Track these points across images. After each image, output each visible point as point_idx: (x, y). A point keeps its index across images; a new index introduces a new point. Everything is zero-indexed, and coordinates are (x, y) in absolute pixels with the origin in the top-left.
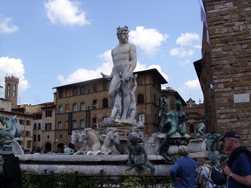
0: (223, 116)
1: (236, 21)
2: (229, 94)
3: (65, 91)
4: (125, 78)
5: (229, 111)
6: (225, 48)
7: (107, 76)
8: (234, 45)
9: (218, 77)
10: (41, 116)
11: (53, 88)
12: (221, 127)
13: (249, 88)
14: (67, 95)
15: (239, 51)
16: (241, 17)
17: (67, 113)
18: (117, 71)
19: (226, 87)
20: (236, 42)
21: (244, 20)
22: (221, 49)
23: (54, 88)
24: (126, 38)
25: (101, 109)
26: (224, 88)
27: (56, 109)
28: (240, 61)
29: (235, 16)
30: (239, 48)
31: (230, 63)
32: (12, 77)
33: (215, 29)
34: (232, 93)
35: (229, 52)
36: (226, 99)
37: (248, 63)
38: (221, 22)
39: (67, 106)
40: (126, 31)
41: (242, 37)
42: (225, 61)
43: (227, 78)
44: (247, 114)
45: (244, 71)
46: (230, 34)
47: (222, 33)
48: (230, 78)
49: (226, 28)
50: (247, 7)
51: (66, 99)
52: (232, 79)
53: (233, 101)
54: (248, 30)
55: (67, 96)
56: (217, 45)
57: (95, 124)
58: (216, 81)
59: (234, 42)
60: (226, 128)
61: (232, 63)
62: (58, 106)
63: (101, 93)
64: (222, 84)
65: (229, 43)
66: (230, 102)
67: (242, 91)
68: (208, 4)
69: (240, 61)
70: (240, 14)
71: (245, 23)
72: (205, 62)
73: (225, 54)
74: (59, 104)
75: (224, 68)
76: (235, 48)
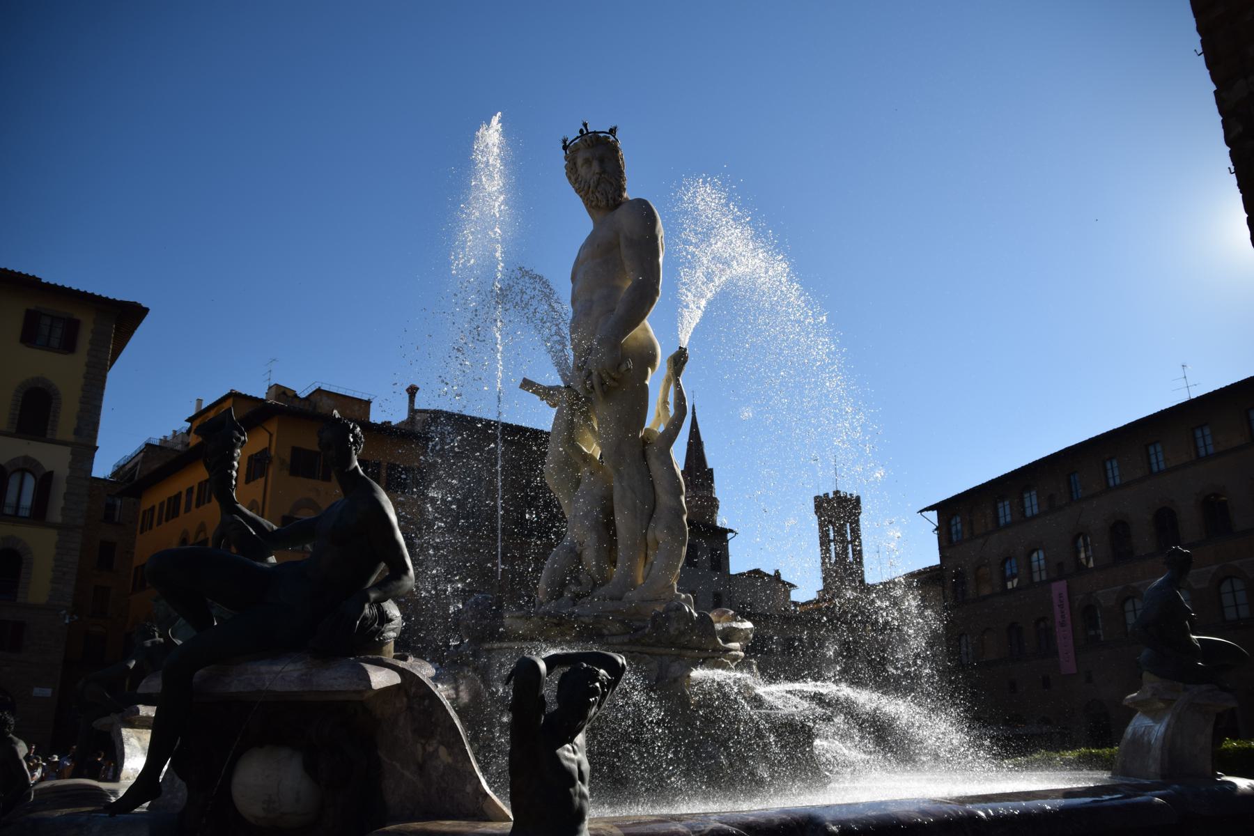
11: (921, 511)
32: (836, 492)
57: (1092, 633)
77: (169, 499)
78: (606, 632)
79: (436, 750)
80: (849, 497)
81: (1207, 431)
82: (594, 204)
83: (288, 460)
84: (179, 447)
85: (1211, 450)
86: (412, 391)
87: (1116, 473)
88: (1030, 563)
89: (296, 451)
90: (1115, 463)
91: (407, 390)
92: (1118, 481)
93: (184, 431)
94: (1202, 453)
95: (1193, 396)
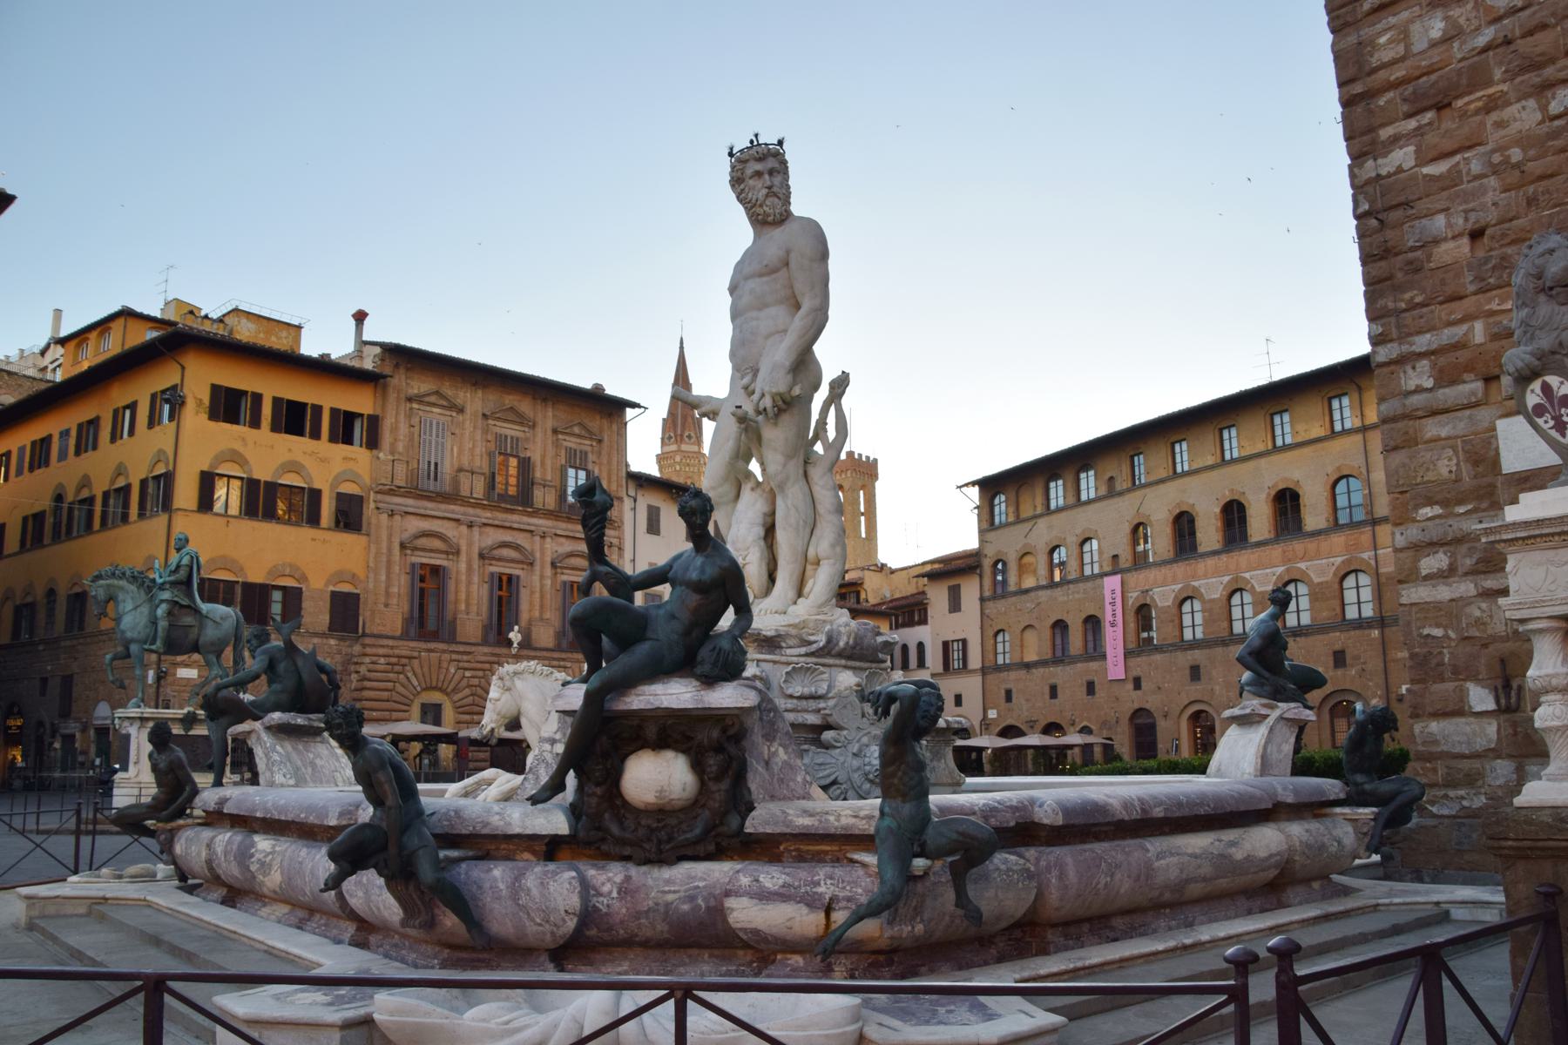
0: (1434, 562)
2: (1470, 417)
3: (1014, 493)
6: (1431, 138)
7: (710, 399)
8: (1495, 108)
9: (1398, 327)
10: (926, 610)
11: (960, 487)
12: (1426, 631)
14: (1022, 507)
15: (1524, 141)
17: (1027, 591)
19: (1446, 378)
22: (1411, 149)
23: (966, 485)
24: (767, 196)
25: (1165, 563)
26: (1440, 383)
27: (981, 576)
28: (1531, 202)
31: (1469, 226)
33: (1372, 43)
34: (1483, 414)
35: (1458, 157)
36: (1450, 452)
39: (1027, 559)
40: (761, 159)
42: (1440, 221)
46: (1467, 47)
47: (1419, 45)
48: (1468, 318)
51: (1020, 526)
52: (1487, 327)
55: (1023, 515)
56: (1385, 133)
57: (1145, 635)
60: (1452, 634)
61: (1483, 223)
62: (987, 564)
63: (1162, 486)
64: (1425, 362)
65: (1460, 103)
66: (1480, 469)
69: (1531, 202)
74: (991, 552)
75: (1432, 265)
77: (34, 443)
78: (784, 645)
79: (777, 750)
80: (864, 459)
81: (1286, 417)
82: (760, 217)
83: (206, 400)
84: (31, 372)
85: (1288, 440)
86: (360, 317)
87: (1185, 457)
88: (1082, 553)
89: (215, 389)
90: (1184, 445)
91: (353, 316)
92: (1186, 468)
93: (37, 350)
94: (1279, 442)
95: (1277, 377)
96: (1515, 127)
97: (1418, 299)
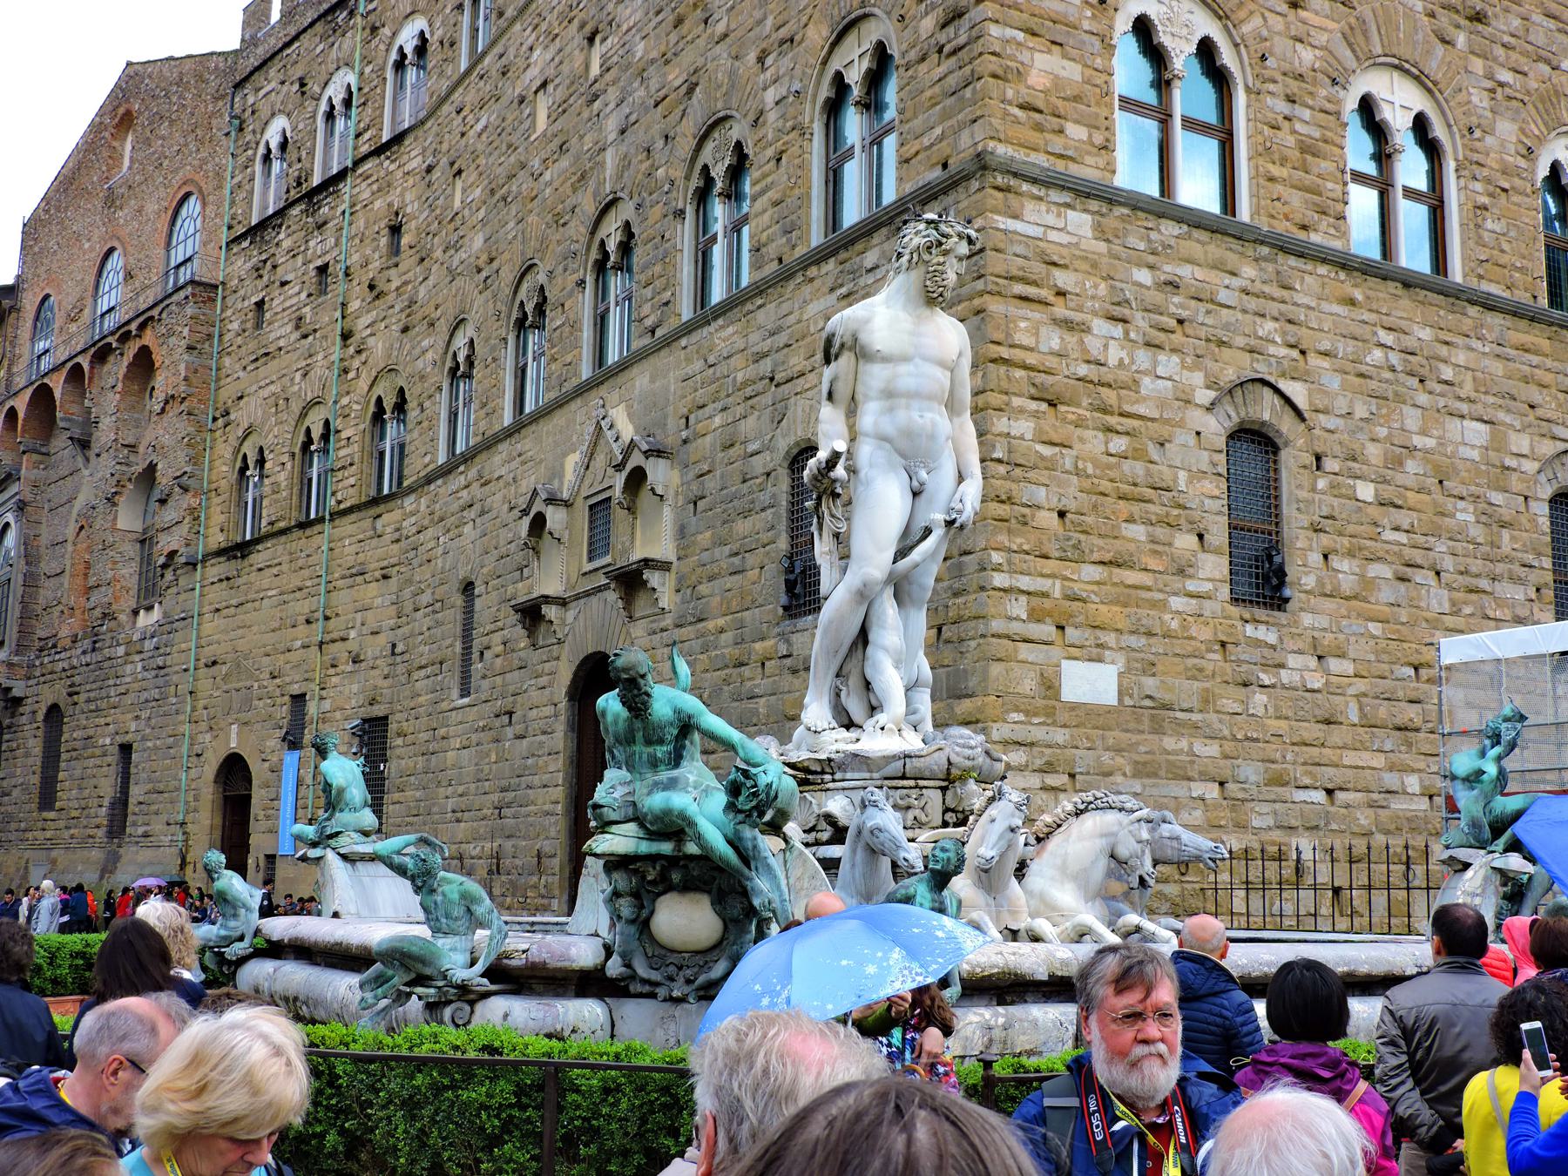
1: (1095, 313)
4: (960, 512)
5: (1038, 734)
9: (1009, 562)
13: (1118, 640)
16: (1116, 299)
18: (903, 455)
19: (1036, 616)
20: (1088, 414)
21: (1125, 321)
22: (1032, 425)
29: (1096, 286)
30: (1094, 442)
31: (1060, 507)
34: (1056, 652)
35: (1057, 449)
36: (1032, 674)
37: (1124, 525)
38: (1044, 293)
41: (1109, 396)
43: (1043, 575)
44: (1106, 758)
45: (1107, 557)
46: (1072, 369)
49: (1058, 330)
50: (1139, 265)
52: (1063, 587)
53: (1057, 697)
54: (1137, 372)
56: (1017, 402)
58: (999, 580)
59: (1080, 411)
65: (1062, 408)
67: (1095, 651)
68: (999, 179)
69: (1095, 507)
70: (1112, 287)
71: (1127, 333)
72: (142, 327)
73: (1042, 458)
76: (1081, 440)
96: (1088, 447)
97: (1026, 547)
